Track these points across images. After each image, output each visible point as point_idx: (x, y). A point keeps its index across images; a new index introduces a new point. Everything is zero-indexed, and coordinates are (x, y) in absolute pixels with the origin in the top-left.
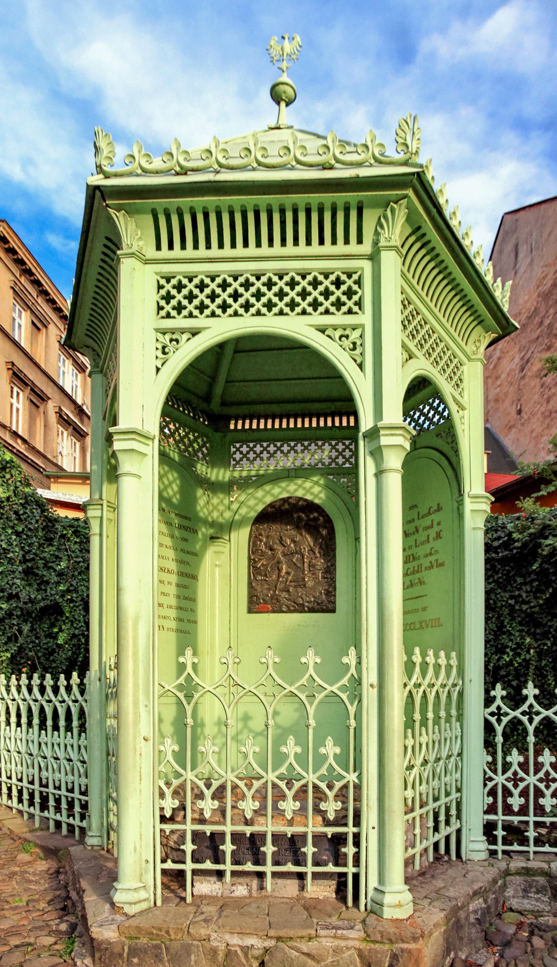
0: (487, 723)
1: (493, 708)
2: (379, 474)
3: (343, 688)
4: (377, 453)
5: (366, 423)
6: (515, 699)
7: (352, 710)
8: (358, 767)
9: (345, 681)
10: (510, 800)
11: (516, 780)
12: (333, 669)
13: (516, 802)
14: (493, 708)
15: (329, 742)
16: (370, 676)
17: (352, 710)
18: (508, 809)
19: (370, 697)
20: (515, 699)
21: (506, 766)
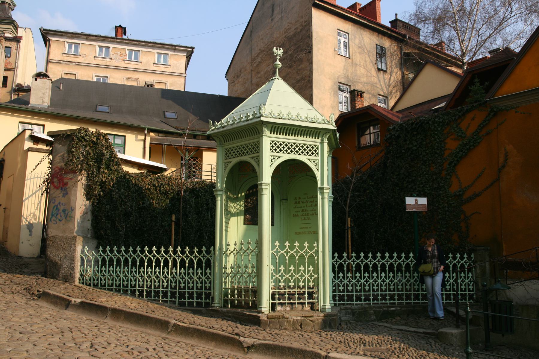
0: (333, 264)
1: (335, 260)
2: (323, 198)
3: (314, 252)
4: (323, 193)
5: (319, 185)
6: (341, 257)
7: (316, 258)
8: (318, 273)
9: (314, 251)
10: (340, 288)
11: (341, 281)
12: (311, 248)
13: (341, 288)
14: (335, 260)
15: (311, 266)
16: (321, 249)
17: (316, 258)
18: (339, 291)
19: (321, 255)
20: (341, 257)
21: (339, 277)
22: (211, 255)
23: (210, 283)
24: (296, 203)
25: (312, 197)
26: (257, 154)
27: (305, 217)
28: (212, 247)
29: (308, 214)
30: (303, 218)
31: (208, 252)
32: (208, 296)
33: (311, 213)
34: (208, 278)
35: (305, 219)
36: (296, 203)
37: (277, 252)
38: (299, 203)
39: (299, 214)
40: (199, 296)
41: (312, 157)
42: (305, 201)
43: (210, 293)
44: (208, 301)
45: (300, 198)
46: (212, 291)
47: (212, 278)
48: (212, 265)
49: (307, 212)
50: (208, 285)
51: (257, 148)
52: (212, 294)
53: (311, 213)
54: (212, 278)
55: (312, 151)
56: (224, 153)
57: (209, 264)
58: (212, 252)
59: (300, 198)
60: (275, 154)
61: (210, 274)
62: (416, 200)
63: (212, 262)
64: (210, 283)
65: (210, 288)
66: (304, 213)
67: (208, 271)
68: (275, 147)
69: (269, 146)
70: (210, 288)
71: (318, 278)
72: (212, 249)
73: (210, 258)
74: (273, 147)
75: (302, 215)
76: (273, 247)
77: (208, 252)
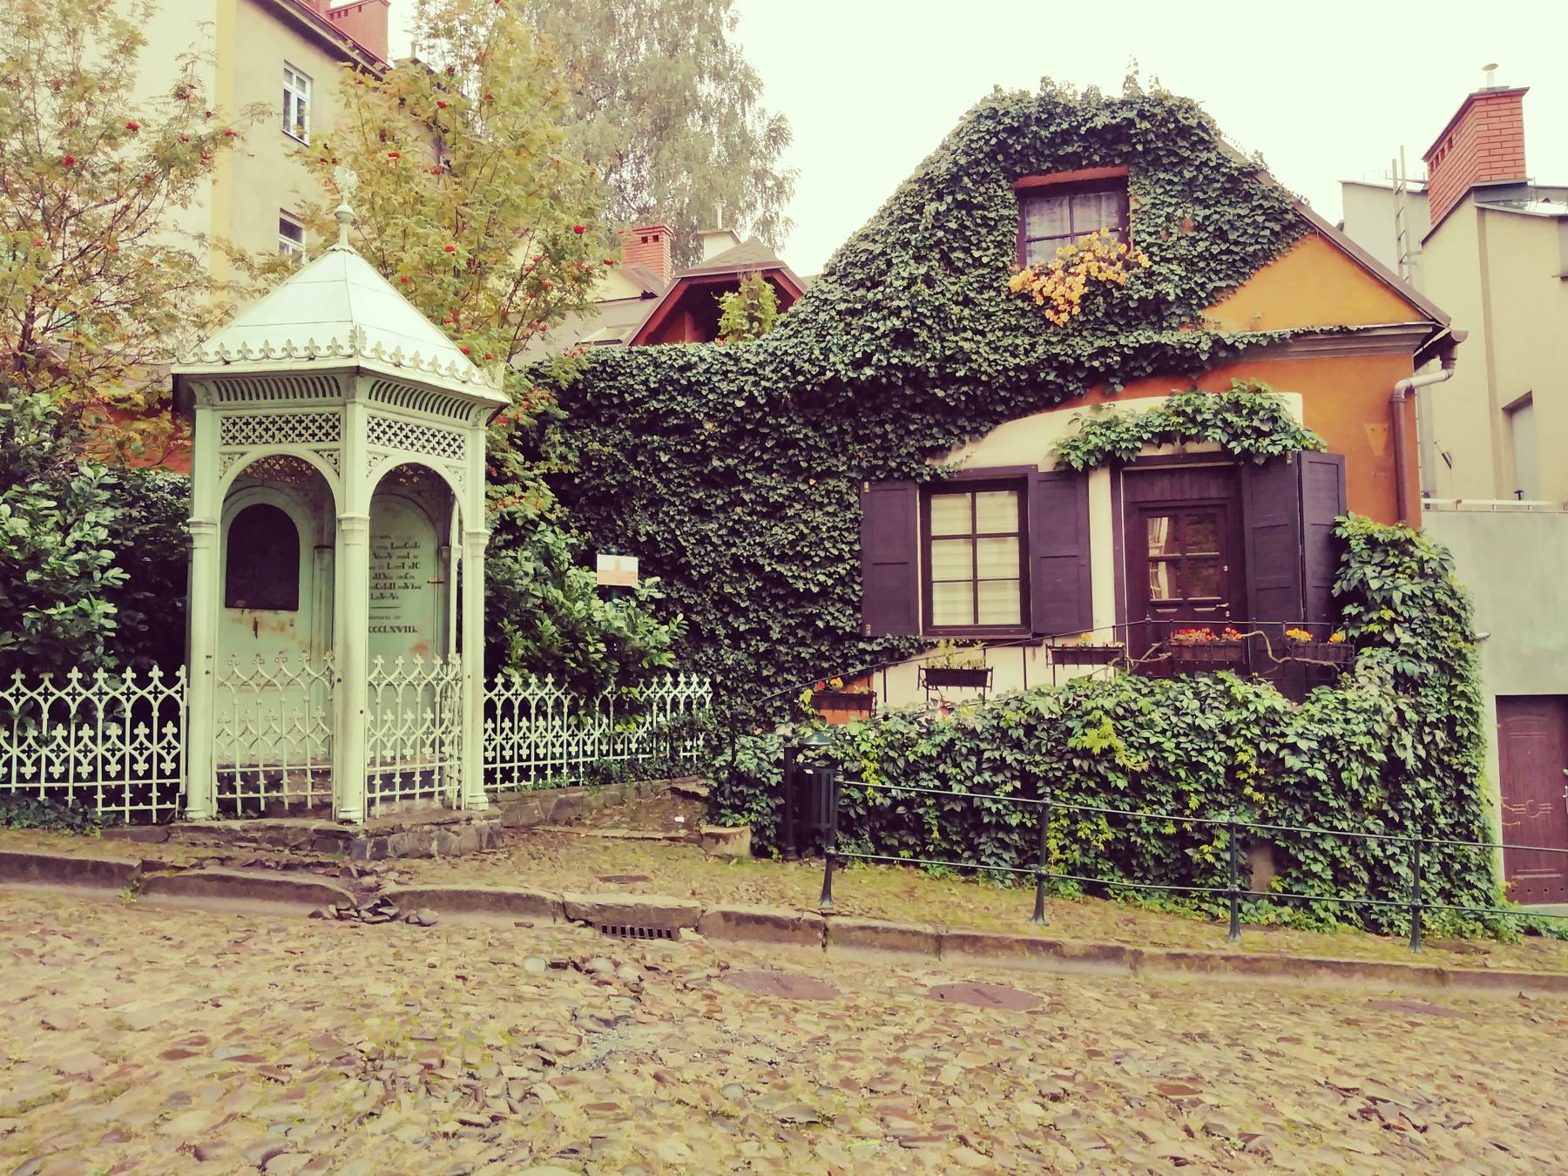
22: (178, 687)
23: (176, 759)
25: (405, 546)
26: (333, 445)
28: (183, 668)
29: (392, 586)
31: (170, 680)
32: (168, 793)
33: (400, 583)
34: (169, 748)
35: (382, 597)
37: (379, 678)
40: (141, 795)
41: (454, 461)
43: (176, 787)
44: (168, 805)
46: (182, 780)
47: (181, 747)
48: (182, 713)
49: (388, 582)
50: (168, 767)
51: (332, 428)
52: (182, 790)
54: (181, 747)
55: (453, 445)
56: (219, 430)
57: (170, 711)
58: (183, 680)
60: (378, 447)
61: (177, 737)
62: (618, 564)
63: (183, 705)
64: (176, 759)
65: (175, 773)
67: (170, 729)
68: (378, 431)
69: (366, 429)
70: (175, 773)
71: (460, 738)
72: (181, 673)
73: (177, 697)
74: (372, 430)
76: (372, 667)
77: (170, 680)
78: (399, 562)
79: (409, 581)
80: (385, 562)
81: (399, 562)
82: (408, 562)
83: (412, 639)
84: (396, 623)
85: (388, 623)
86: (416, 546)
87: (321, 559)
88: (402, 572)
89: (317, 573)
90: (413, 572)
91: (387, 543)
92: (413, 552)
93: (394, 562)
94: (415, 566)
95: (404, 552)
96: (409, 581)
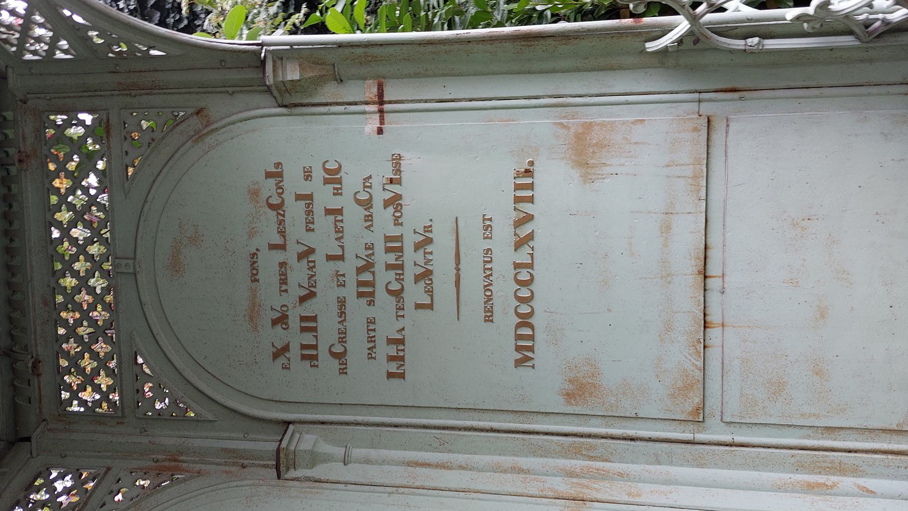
24: (310, 356)
27: (410, 272)
29: (394, 245)
30: (414, 293)
33: (383, 216)
35: (426, 275)
36: (310, 356)
38: (309, 324)
39: (387, 328)
42: (298, 274)
45: (281, 320)
49: (382, 258)
53: (383, 216)
59: (281, 320)
66: (384, 277)
75: (397, 294)
78: (325, 224)
79: (379, 196)
80: (324, 269)
81: (325, 224)
82: (324, 197)
83: (555, 180)
84: (504, 232)
85: (505, 257)
86: (276, 175)
87: (315, 459)
88: (353, 215)
89: (353, 472)
90: (351, 182)
91: (269, 262)
92: (294, 183)
93: (323, 241)
94: (333, 177)
95: (295, 211)
96: (379, 196)
